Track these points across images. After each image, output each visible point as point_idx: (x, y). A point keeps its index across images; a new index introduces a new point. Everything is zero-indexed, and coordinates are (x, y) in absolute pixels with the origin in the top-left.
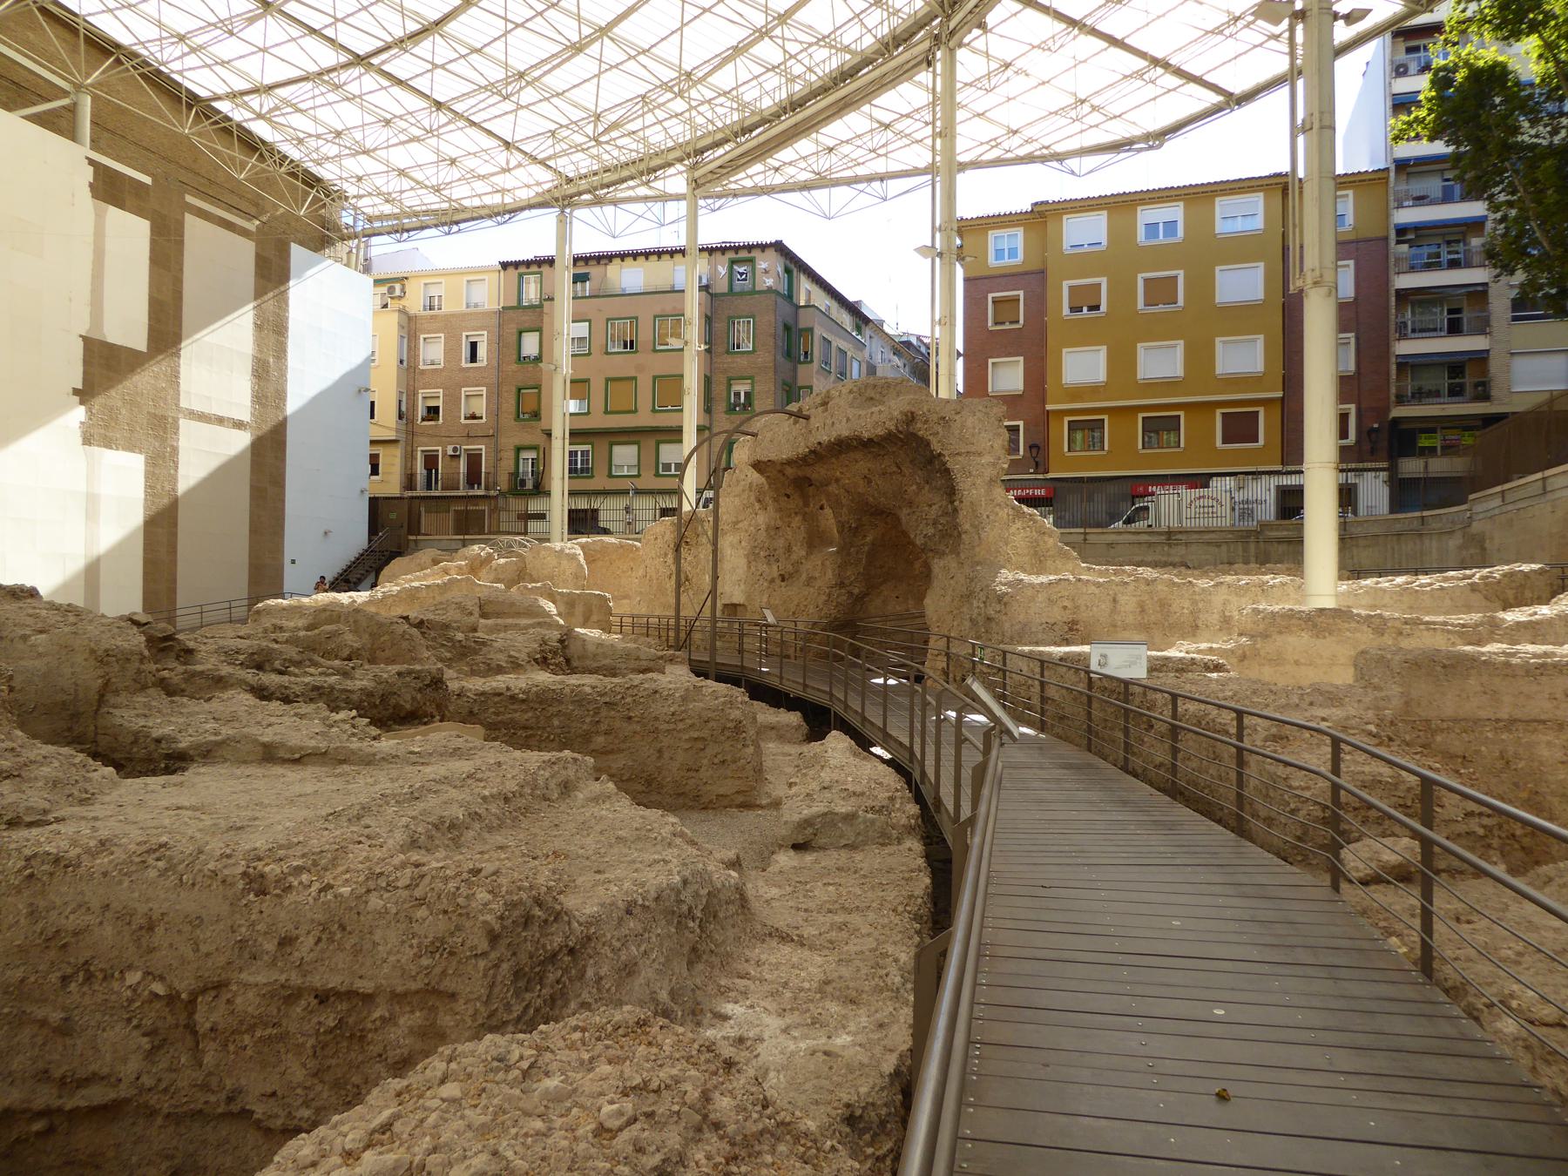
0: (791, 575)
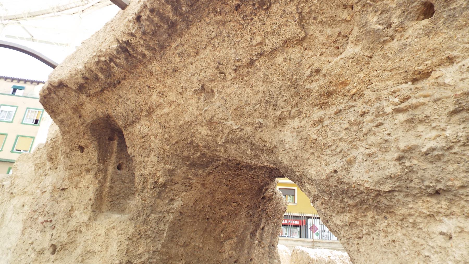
0: (64, 247)
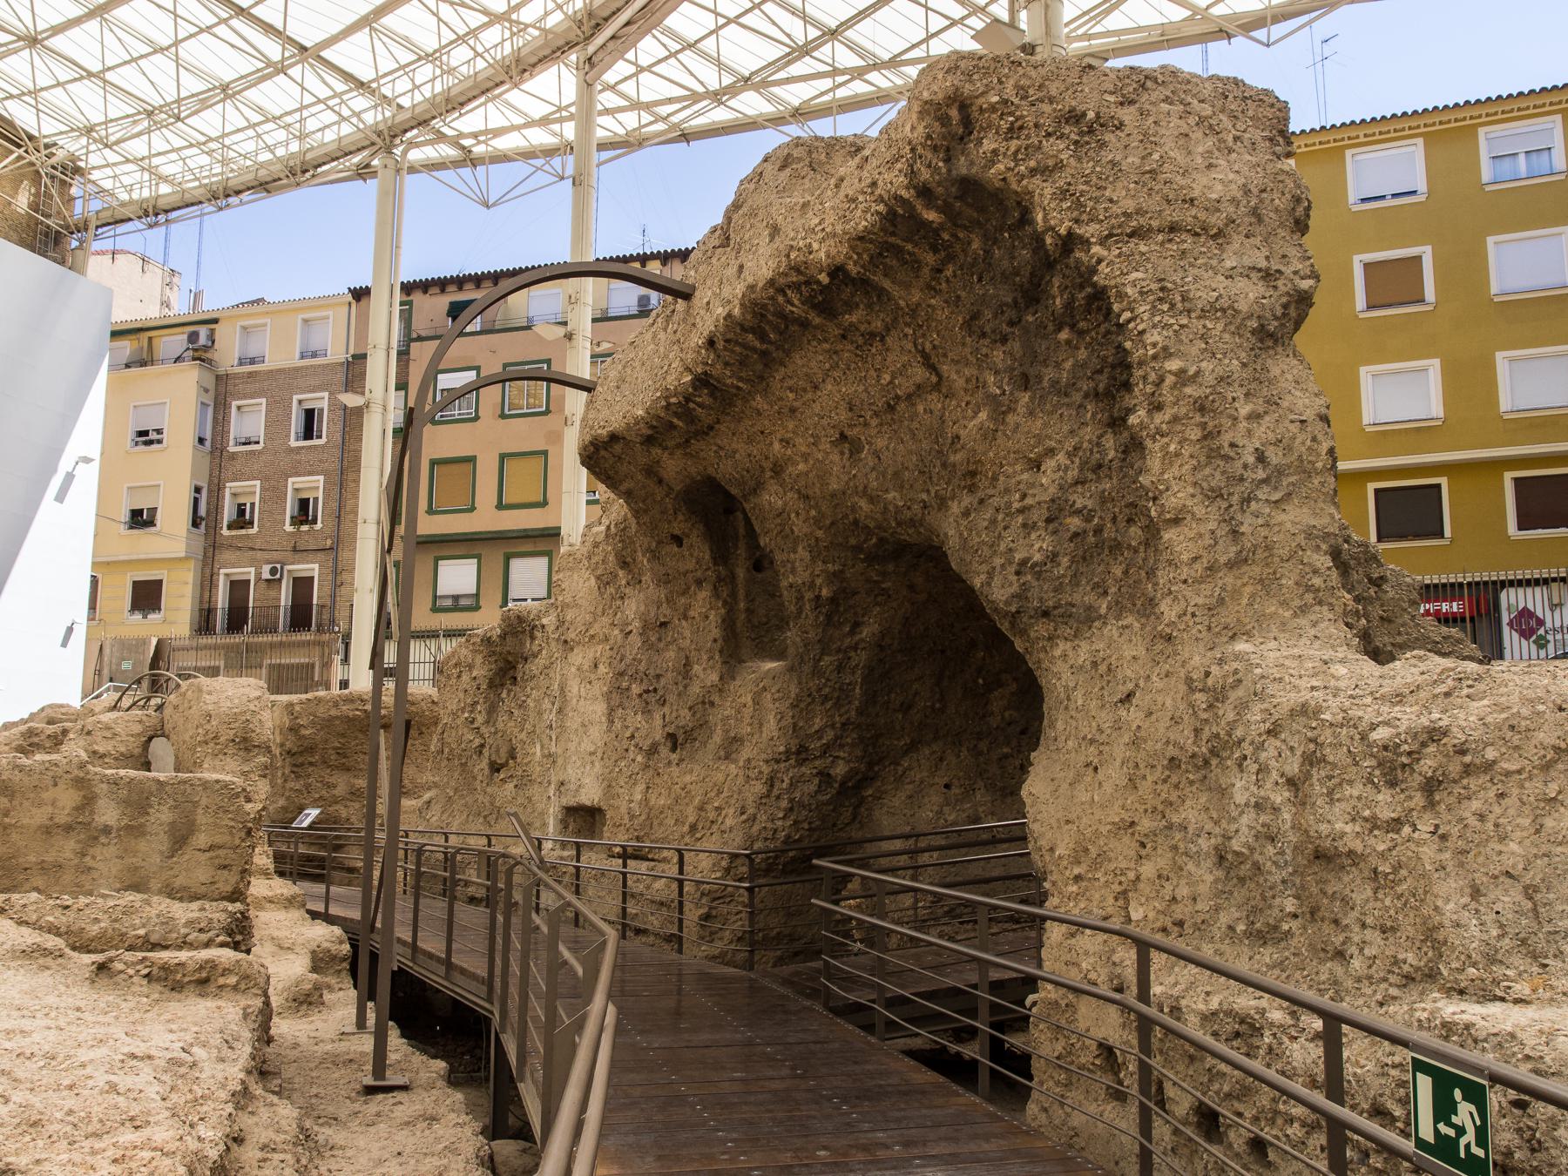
0: (690, 735)
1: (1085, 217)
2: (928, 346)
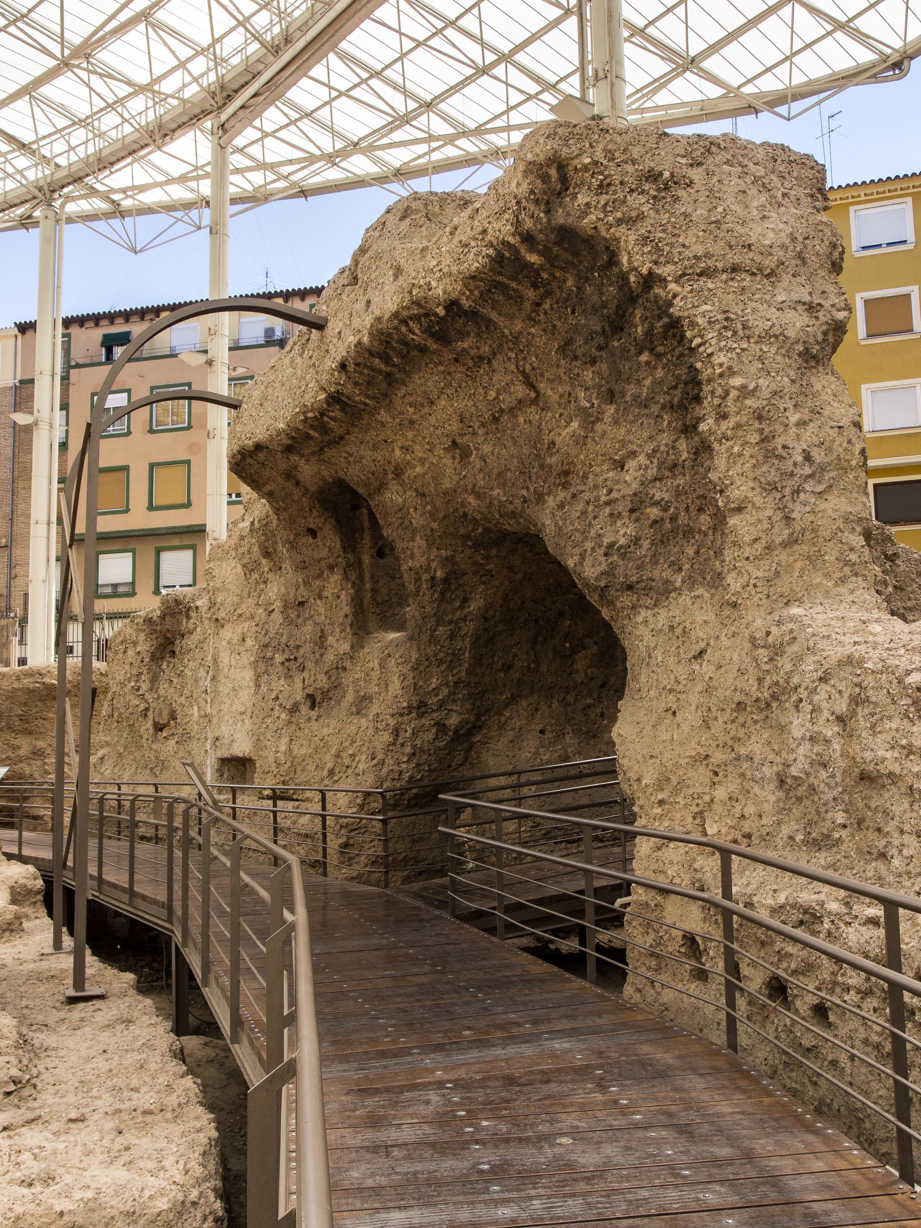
0: (326, 695)
1: (662, 259)
2: (528, 368)
